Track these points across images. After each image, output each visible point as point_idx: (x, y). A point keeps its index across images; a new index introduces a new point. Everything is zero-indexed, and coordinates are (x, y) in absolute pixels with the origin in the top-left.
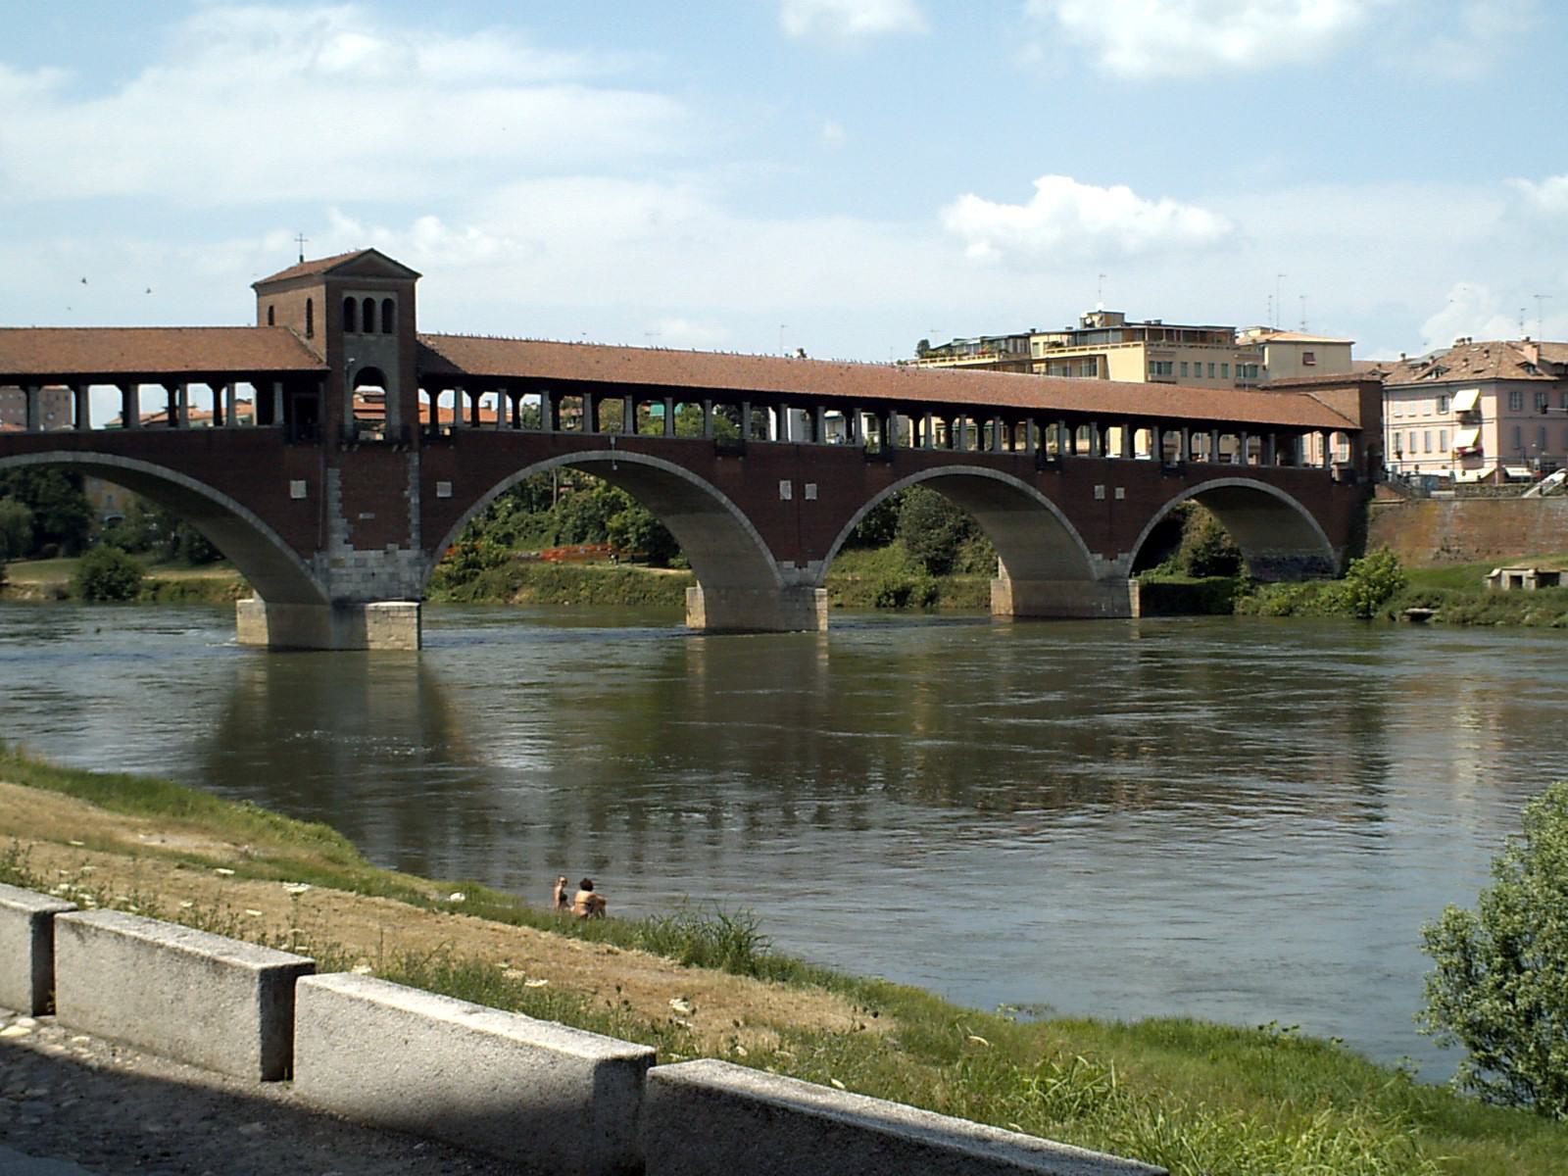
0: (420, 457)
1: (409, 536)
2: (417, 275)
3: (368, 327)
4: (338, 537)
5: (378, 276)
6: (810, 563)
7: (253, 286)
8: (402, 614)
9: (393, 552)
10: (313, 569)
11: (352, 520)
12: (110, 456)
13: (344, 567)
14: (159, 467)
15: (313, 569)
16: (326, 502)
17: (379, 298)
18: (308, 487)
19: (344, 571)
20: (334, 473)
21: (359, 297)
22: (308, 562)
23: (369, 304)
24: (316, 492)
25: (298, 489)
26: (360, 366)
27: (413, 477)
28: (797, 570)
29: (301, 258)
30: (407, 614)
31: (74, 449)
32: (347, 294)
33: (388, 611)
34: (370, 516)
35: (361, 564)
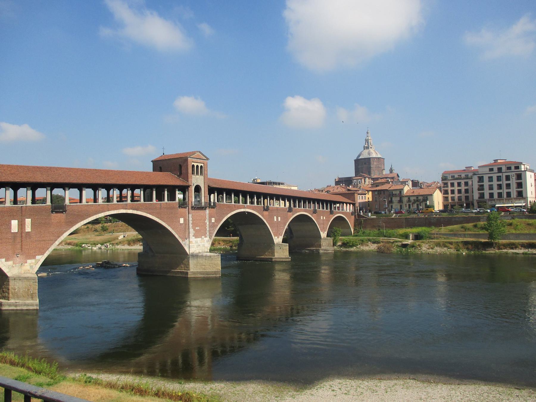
2: (208, 159)
3: (197, 174)
4: (191, 235)
5: (200, 159)
6: (280, 237)
7: (152, 161)
8: (215, 257)
9: (203, 238)
10: (185, 244)
11: (194, 230)
12: (136, 211)
13: (193, 243)
14: (148, 215)
15: (185, 244)
16: (189, 224)
17: (200, 165)
18: (185, 220)
19: (192, 245)
20: (190, 215)
22: (184, 242)
23: (197, 166)
24: (186, 221)
25: (182, 221)
26: (195, 185)
27: (207, 216)
29: (164, 154)
30: (217, 257)
31: (126, 209)
32: (193, 163)
33: (210, 256)
34: (198, 228)
35: (196, 242)
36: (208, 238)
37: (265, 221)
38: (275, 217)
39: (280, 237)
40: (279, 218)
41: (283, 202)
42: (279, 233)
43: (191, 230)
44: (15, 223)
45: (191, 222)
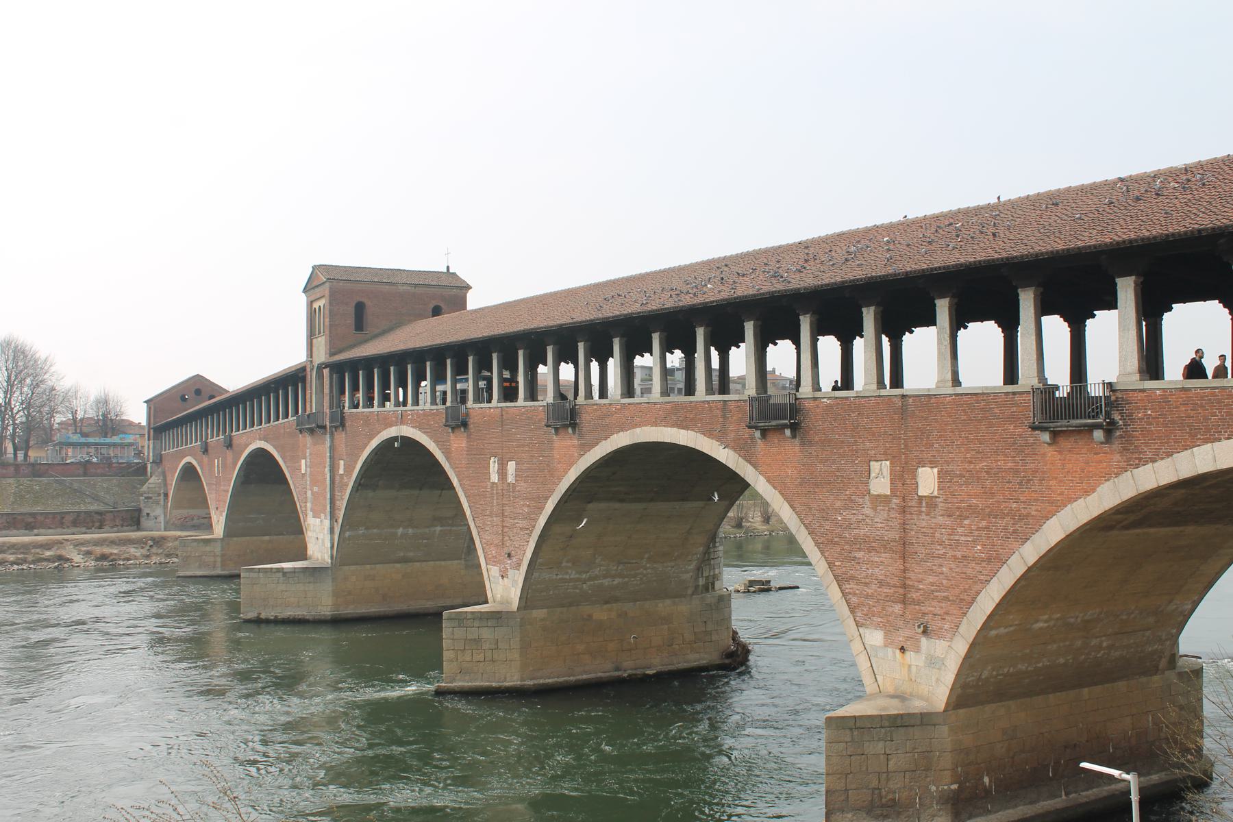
11: (313, 494)
29: (448, 268)
36: (327, 523)
37: (455, 482)
38: (494, 466)
39: (511, 573)
40: (511, 466)
41: (571, 366)
42: (506, 550)
43: (309, 493)
44: (216, 460)
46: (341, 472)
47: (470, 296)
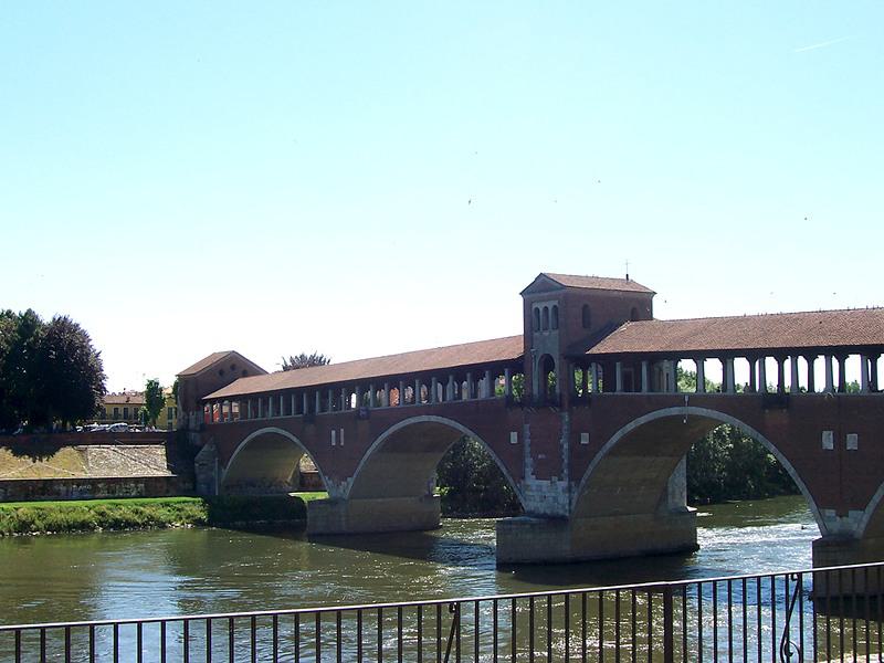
0: (570, 416)
1: (562, 472)
4: (529, 470)
6: (850, 513)
11: (535, 459)
13: (531, 490)
21: (541, 306)
25: (514, 438)
26: (541, 354)
28: (838, 518)
32: (534, 307)
34: (544, 456)
35: (539, 488)
36: (564, 484)
39: (850, 513)
43: (529, 460)
44: (333, 432)
45: (528, 441)
46: (585, 441)
47: (656, 301)
